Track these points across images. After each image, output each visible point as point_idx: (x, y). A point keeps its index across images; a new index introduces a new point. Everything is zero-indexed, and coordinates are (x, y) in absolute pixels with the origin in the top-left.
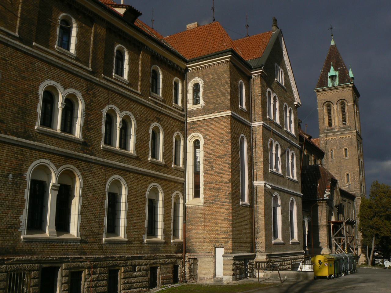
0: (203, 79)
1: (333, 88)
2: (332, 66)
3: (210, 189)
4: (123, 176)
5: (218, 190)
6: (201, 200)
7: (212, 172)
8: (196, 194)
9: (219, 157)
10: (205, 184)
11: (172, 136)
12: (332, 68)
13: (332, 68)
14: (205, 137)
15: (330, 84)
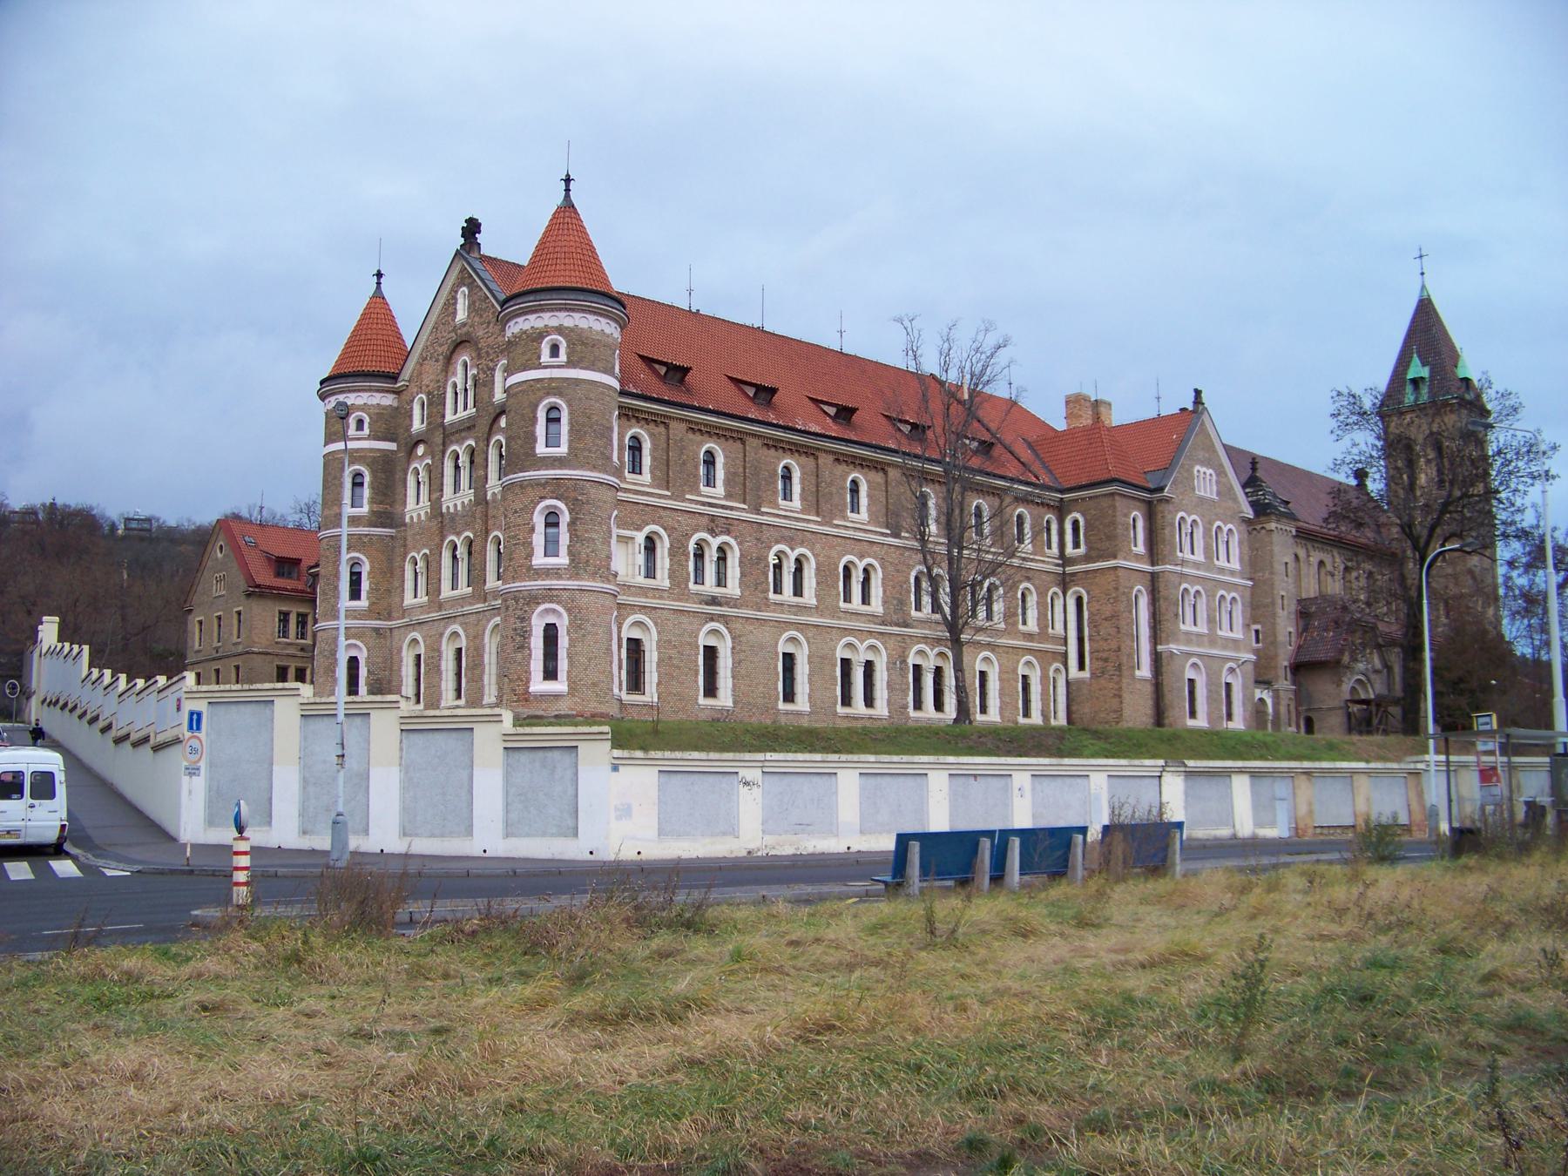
0: (1083, 515)
1: (1417, 408)
2: (1415, 355)
3: (1097, 659)
4: (993, 651)
5: (1106, 660)
6: (1086, 674)
7: (1098, 638)
8: (1081, 667)
9: (1106, 619)
10: (1091, 653)
11: (1047, 595)
12: (1416, 360)
13: (1416, 360)
14: (1088, 593)
15: (1409, 398)
